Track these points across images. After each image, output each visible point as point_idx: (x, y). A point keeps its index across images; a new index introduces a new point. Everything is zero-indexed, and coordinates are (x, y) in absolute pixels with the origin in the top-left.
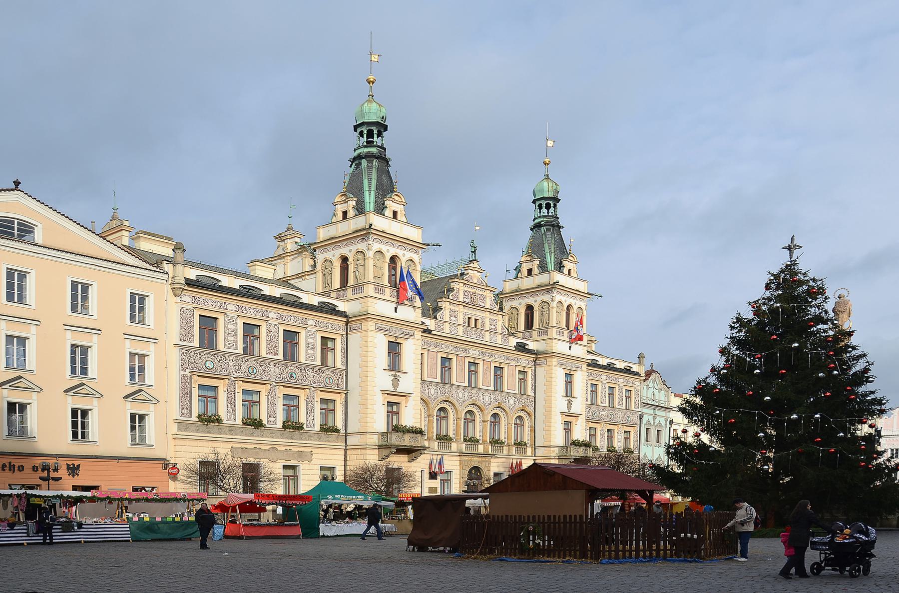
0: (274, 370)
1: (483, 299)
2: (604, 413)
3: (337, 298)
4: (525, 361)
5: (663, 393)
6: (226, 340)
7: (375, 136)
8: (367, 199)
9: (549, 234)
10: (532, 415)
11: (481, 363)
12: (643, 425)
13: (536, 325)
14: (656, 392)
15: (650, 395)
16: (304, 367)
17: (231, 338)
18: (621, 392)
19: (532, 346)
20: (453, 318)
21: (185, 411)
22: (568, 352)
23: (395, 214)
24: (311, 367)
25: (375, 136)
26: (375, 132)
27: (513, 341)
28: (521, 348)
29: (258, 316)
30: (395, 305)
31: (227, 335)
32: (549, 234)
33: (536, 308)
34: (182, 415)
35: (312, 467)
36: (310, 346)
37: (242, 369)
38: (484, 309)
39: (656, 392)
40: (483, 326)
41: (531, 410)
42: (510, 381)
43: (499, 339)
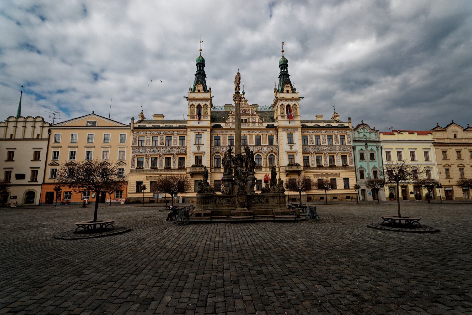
0: (162, 150)
1: (249, 111)
2: (325, 148)
4: (271, 132)
10: (278, 153)
11: (248, 136)
16: (173, 147)
18: (336, 137)
22: (198, 125)
24: (175, 147)
27: (265, 125)
29: (157, 134)
30: (198, 122)
34: (132, 167)
36: (175, 140)
38: (249, 115)
41: (277, 151)
42: (265, 141)
43: (257, 125)
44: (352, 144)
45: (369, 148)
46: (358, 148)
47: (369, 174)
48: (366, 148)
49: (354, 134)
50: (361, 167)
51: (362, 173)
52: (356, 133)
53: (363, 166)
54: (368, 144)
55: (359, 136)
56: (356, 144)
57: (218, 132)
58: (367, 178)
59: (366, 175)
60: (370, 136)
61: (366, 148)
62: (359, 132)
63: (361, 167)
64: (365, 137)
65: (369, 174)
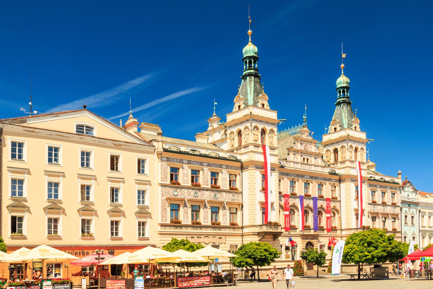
0: (207, 193)
3: (237, 153)
5: (414, 194)
6: (183, 179)
7: (253, 63)
8: (249, 98)
9: (345, 107)
12: (403, 214)
13: (339, 160)
14: (410, 194)
15: (407, 196)
17: (186, 178)
19: (337, 172)
20: (295, 159)
21: (164, 218)
23: (263, 105)
25: (253, 63)
26: (253, 61)
28: (333, 174)
31: (184, 176)
32: (345, 107)
33: (339, 150)
35: (226, 245)
36: (224, 180)
37: (191, 194)
39: (410, 194)
40: (311, 162)
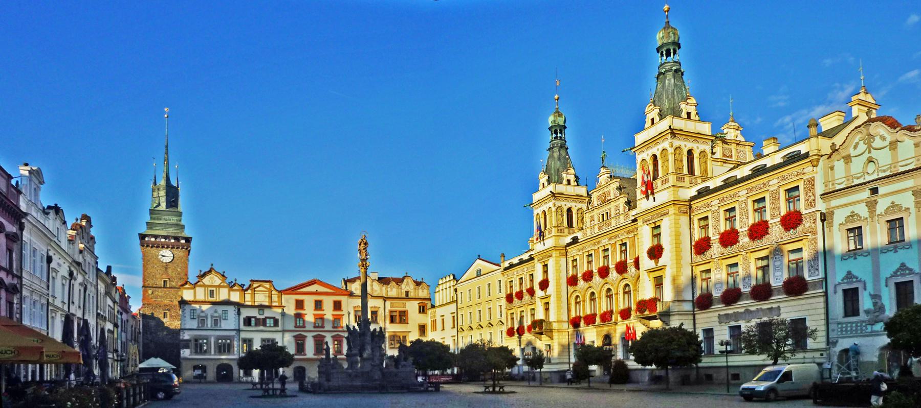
44: (821, 206)
45: (882, 205)
46: (839, 217)
47: (876, 297)
48: (872, 205)
49: (832, 168)
50: (849, 276)
51: (851, 297)
52: (839, 165)
53: (855, 273)
54: (882, 191)
55: (848, 170)
56: (834, 203)
57: (572, 250)
58: (867, 312)
59: (865, 303)
60: (894, 157)
61: (872, 205)
62: (848, 159)
63: (849, 276)
64: (871, 168)
65: (876, 297)
